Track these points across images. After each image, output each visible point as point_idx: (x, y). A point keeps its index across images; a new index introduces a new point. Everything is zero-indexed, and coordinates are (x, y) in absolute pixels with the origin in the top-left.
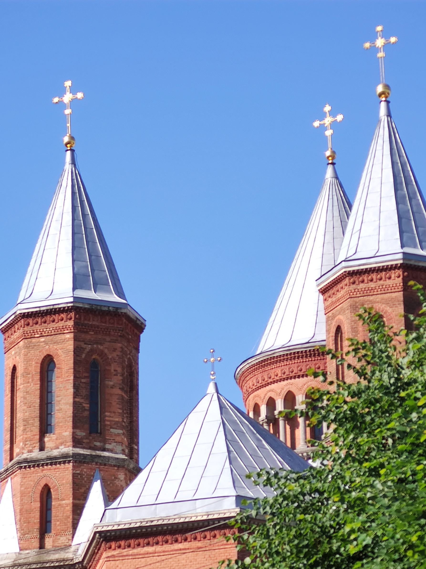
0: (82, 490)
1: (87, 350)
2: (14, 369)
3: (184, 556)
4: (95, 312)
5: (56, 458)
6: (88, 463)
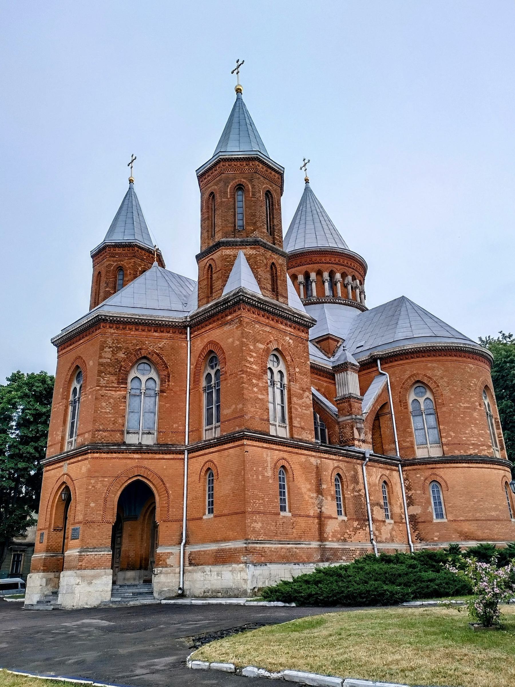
1: (115, 265)
4: (119, 246)
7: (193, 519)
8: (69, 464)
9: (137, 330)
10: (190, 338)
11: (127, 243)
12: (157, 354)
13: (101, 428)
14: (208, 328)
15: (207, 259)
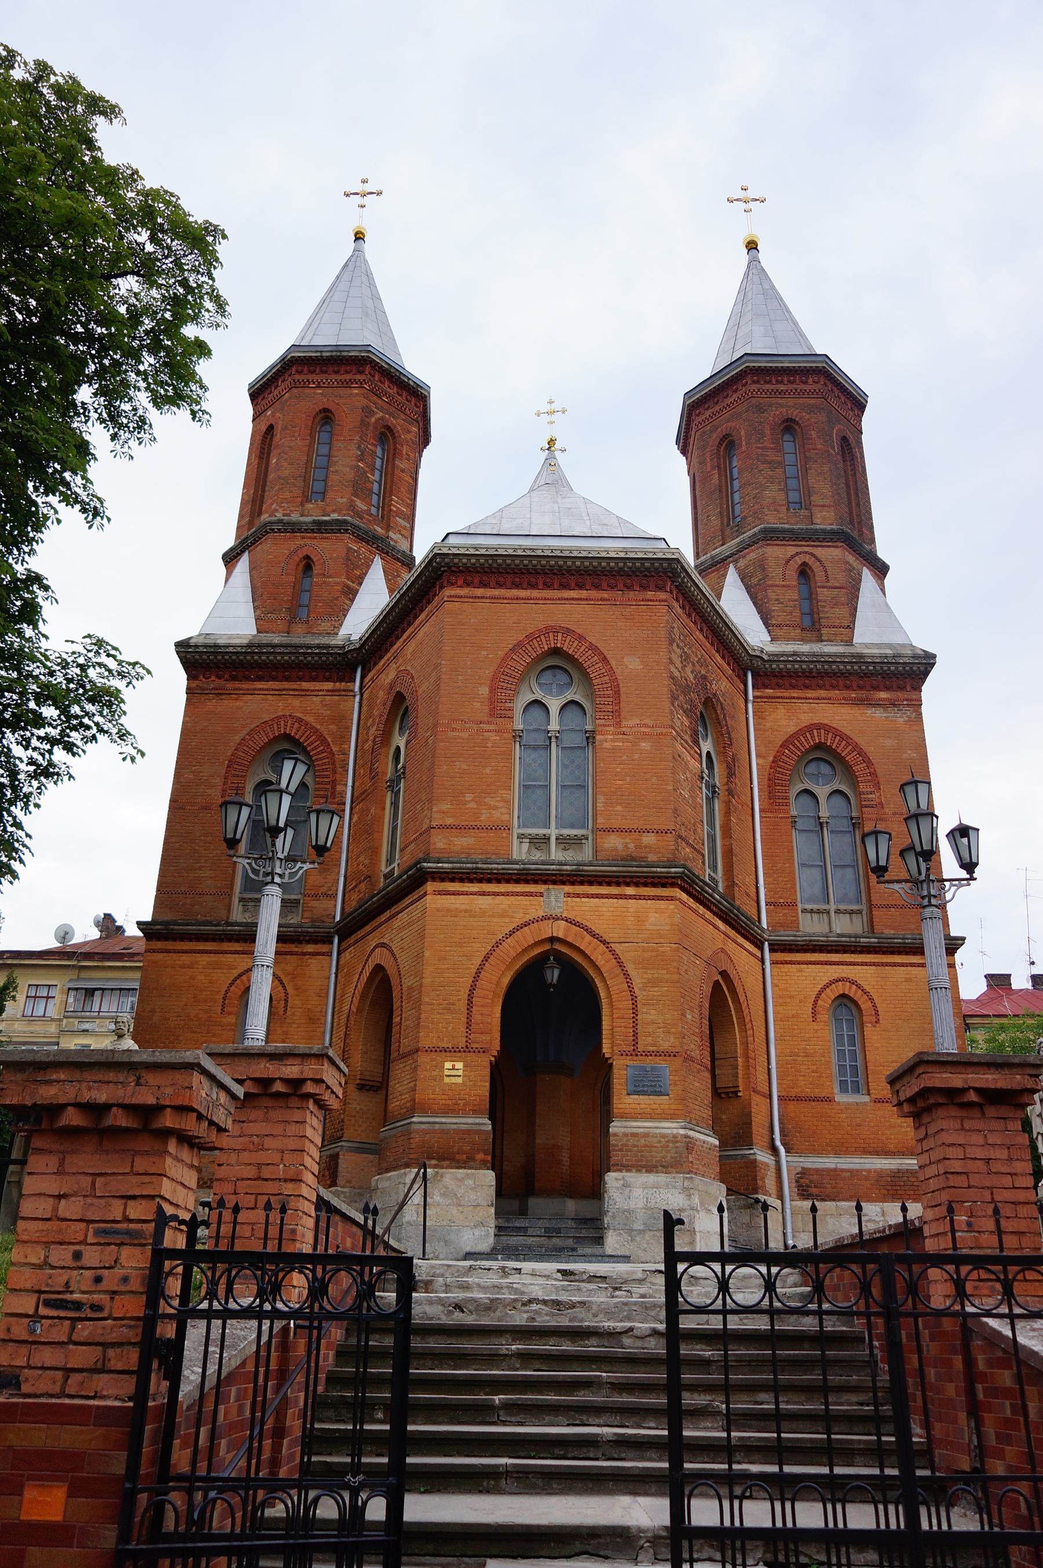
0: (358, 573)
2: (271, 428)
3: (579, 608)
5: (326, 523)
6: (367, 542)
7: (798, 1099)
8: (568, 895)
9: (701, 630)
10: (754, 697)
11: (411, 383)
12: (722, 704)
13: (683, 833)
14: (810, 694)
15: (799, 549)
